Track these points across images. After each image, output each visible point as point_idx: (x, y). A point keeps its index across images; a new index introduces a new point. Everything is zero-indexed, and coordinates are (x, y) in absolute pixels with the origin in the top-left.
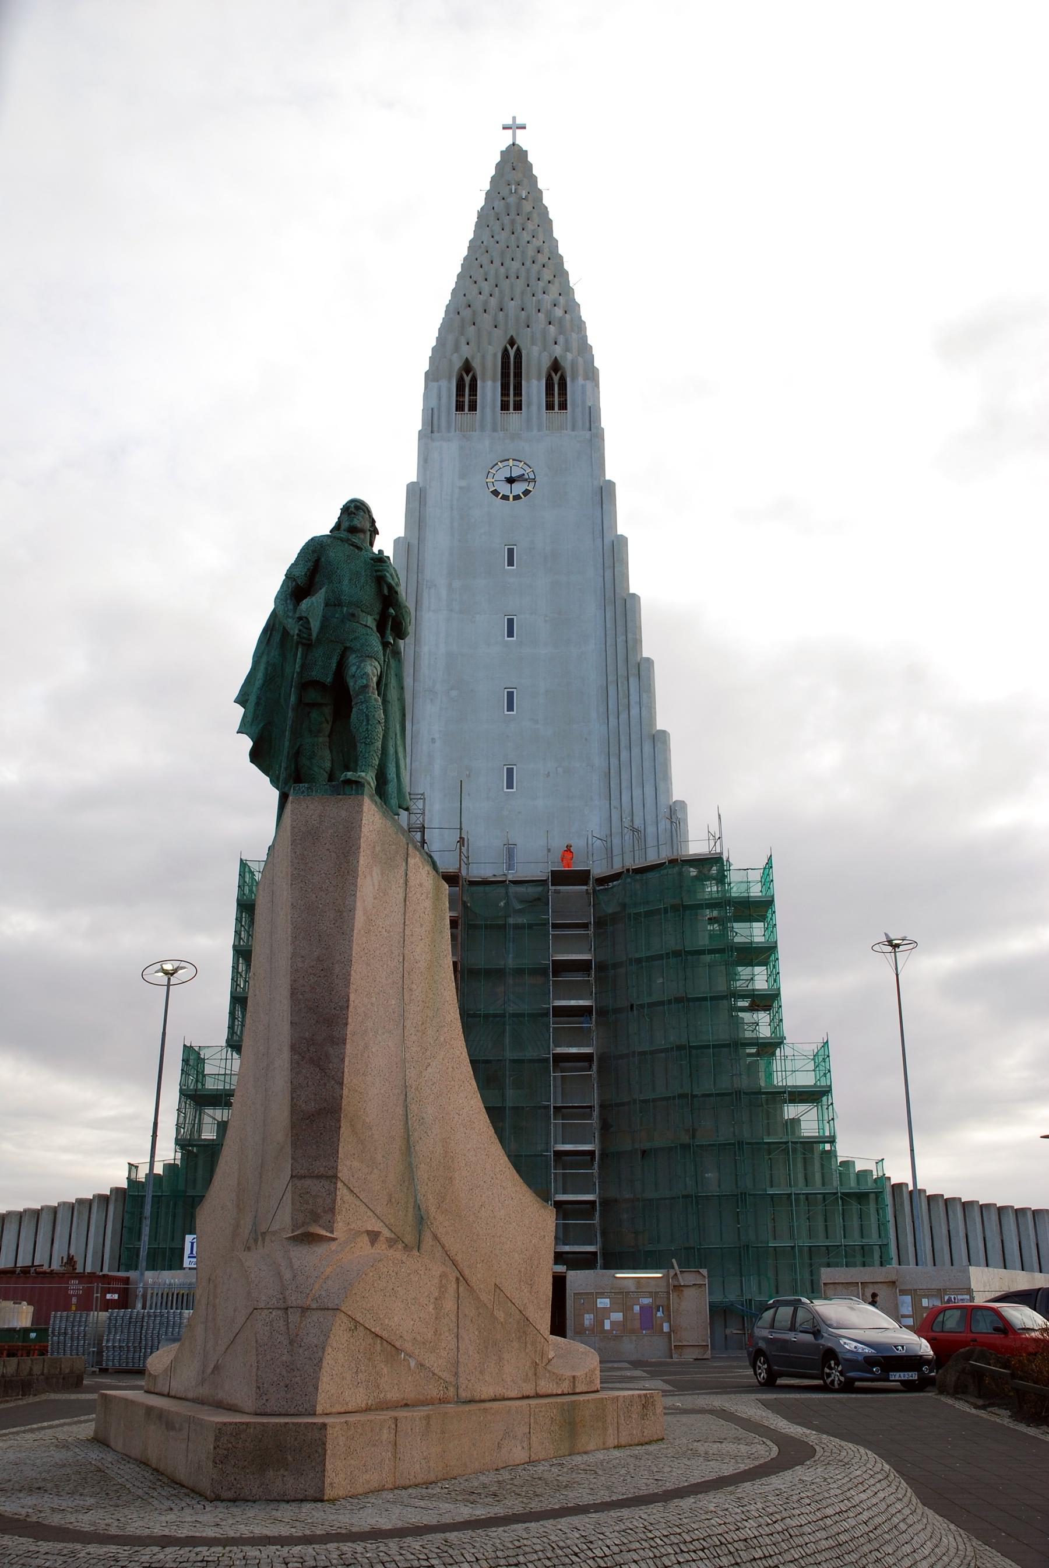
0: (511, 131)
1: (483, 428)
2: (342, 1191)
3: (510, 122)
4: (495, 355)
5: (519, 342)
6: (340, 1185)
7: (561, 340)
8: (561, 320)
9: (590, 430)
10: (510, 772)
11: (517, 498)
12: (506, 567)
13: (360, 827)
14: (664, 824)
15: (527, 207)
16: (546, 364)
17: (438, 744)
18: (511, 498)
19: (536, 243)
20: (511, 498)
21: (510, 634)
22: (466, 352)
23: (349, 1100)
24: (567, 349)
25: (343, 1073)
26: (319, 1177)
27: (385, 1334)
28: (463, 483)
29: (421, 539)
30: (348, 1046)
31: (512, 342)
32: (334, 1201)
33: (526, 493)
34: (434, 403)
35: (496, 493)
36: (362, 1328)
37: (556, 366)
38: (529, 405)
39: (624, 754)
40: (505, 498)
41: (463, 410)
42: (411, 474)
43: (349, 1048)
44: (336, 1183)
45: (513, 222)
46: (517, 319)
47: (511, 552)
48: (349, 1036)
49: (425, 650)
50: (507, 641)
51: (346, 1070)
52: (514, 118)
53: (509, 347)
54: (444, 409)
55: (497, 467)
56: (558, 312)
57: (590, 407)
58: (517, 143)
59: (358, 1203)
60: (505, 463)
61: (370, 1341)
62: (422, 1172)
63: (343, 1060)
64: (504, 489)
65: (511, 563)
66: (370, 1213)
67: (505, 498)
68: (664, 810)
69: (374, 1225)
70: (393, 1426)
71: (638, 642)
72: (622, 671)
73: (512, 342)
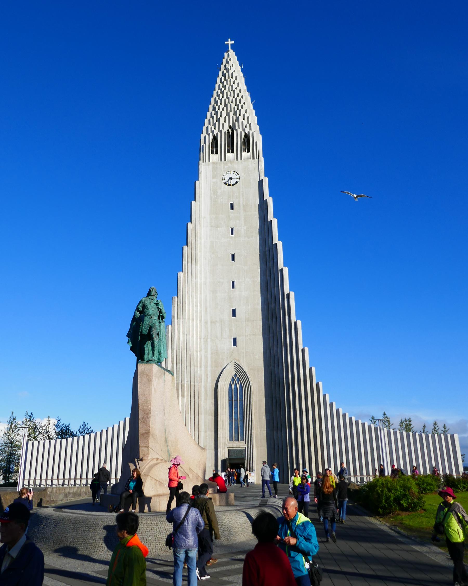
2: (150, 450)
4: (225, 132)
6: (149, 448)
9: (258, 159)
10: (233, 283)
11: (233, 185)
13: (153, 370)
16: (243, 135)
19: (238, 89)
20: (231, 184)
23: (151, 430)
24: (251, 129)
25: (150, 425)
26: (145, 447)
27: (159, 480)
30: (151, 419)
32: (148, 452)
33: (237, 183)
35: (226, 183)
36: (154, 479)
37: (247, 136)
39: (272, 275)
40: (229, 185)
41: (213, 154)
43: (151, 419)
44: (149, 448)
45: (230, 80)
46: (233, 117)
48: (151, 416)
50: (231, 237)
51: (150, 424)
57: (258, 150)
59: (154, 452)
61: (155, 481)
62: (170, 444)
63: (150, 422)
66: (157, 454)
69: (158, 456)
70: (159, 498)
73: (230, 127)
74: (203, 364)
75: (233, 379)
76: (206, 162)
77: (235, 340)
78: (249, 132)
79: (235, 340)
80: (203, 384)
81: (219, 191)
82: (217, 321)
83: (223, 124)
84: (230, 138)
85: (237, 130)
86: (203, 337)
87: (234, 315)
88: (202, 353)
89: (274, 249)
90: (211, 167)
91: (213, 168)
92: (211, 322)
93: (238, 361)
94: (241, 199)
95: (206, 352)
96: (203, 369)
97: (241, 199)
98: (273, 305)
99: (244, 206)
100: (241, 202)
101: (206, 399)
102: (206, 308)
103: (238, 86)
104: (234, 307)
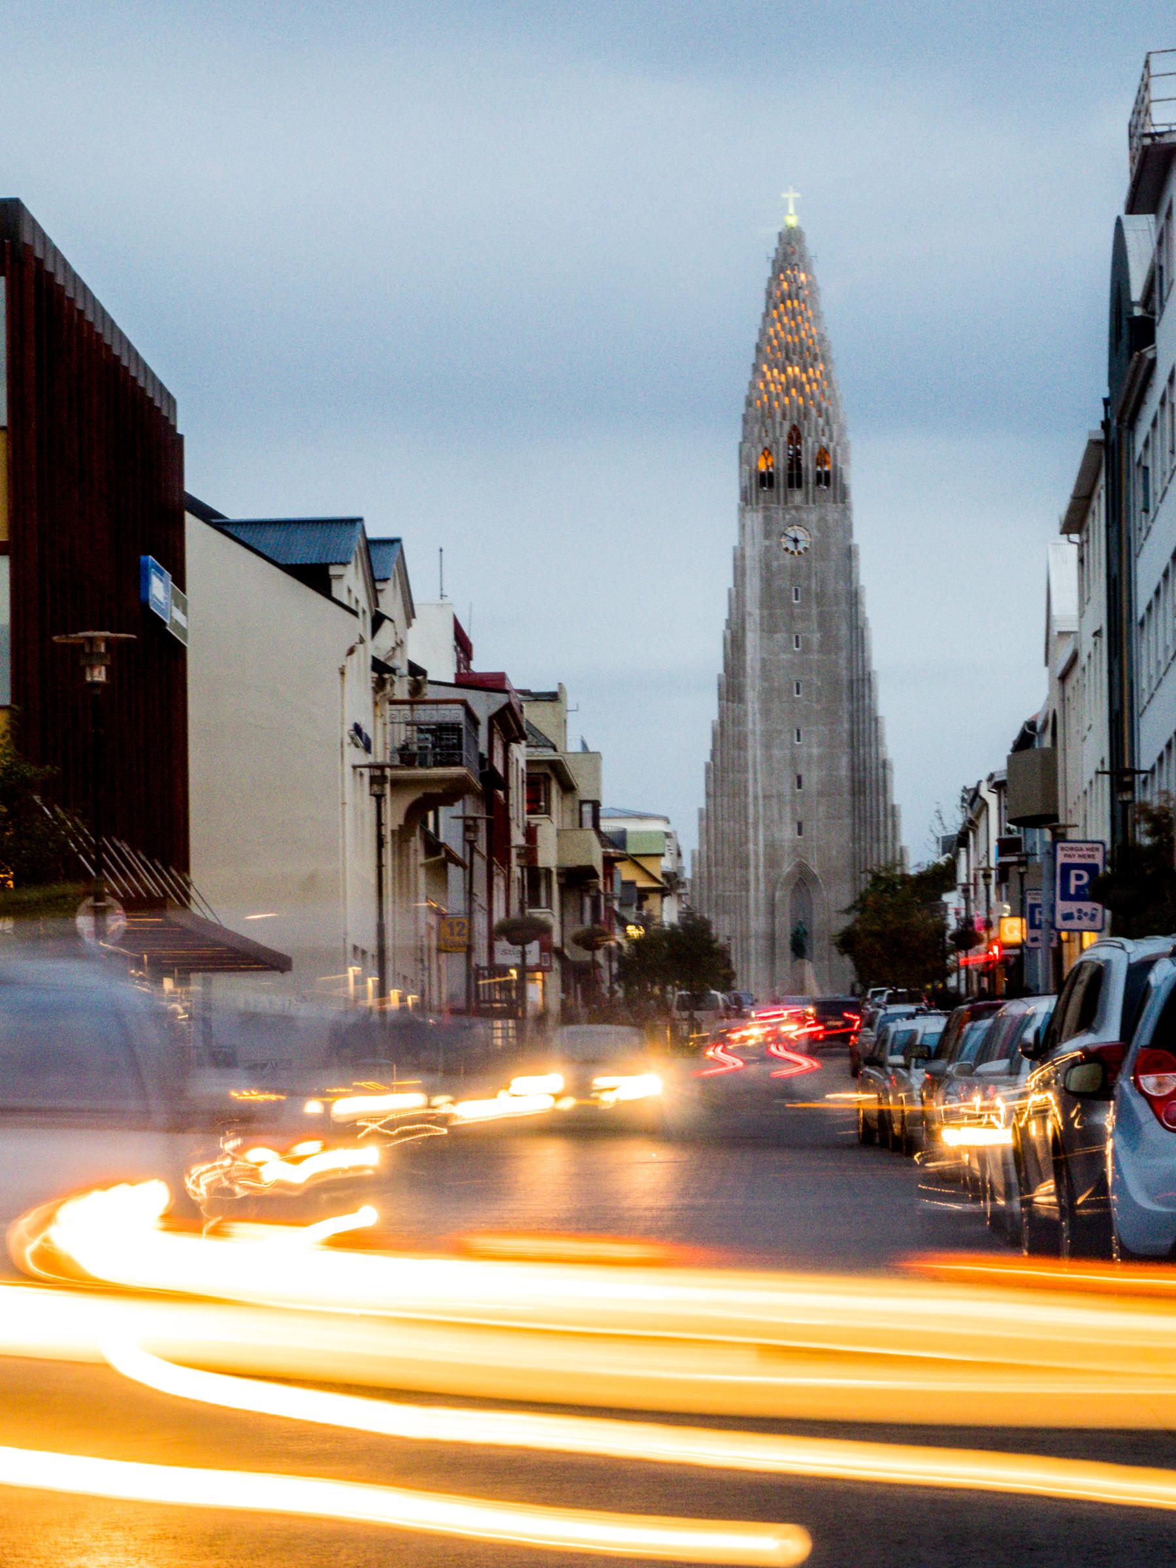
1: (778, 499)
12: (795, 602)
14: (881, 770)
17: (758, 716)
21: (797, 646)
24: (831, 439)
28: (767, 543)
29: (743, 584)
34: (748, 482)
38: (807, 483)
39: (861, 726)
42: (735, 541)
49: (749, 657)
54: (754, 486)
64: (791, 546)
67: (792, 553)
68: (880, 762)
72: (860, 673)
73: (794, 428)
74: (752, 862)
76: (752, 505)
78: (828, 446)
79: (800, 825)
80: (752, 893)
81: (775, 564)
82: (772, 796)
83: (781, 424)
84: (795, 462)
85: (806, 442)
86: (751, 820)
87: (799, 787)
88: (751, 846)
89: (866, 682)
90: (760, 515)
91: (765, 517)
92: (765, 797)
93: (805, 858)
94: (814, 581)
95: (756, 844)
96: (752, 869)
97: (814, 581)
98: (862, 774)
99: (817, 594)
100: (813, 586)
101: (757, 915)
102: (755, 773)
104: (799, 773)
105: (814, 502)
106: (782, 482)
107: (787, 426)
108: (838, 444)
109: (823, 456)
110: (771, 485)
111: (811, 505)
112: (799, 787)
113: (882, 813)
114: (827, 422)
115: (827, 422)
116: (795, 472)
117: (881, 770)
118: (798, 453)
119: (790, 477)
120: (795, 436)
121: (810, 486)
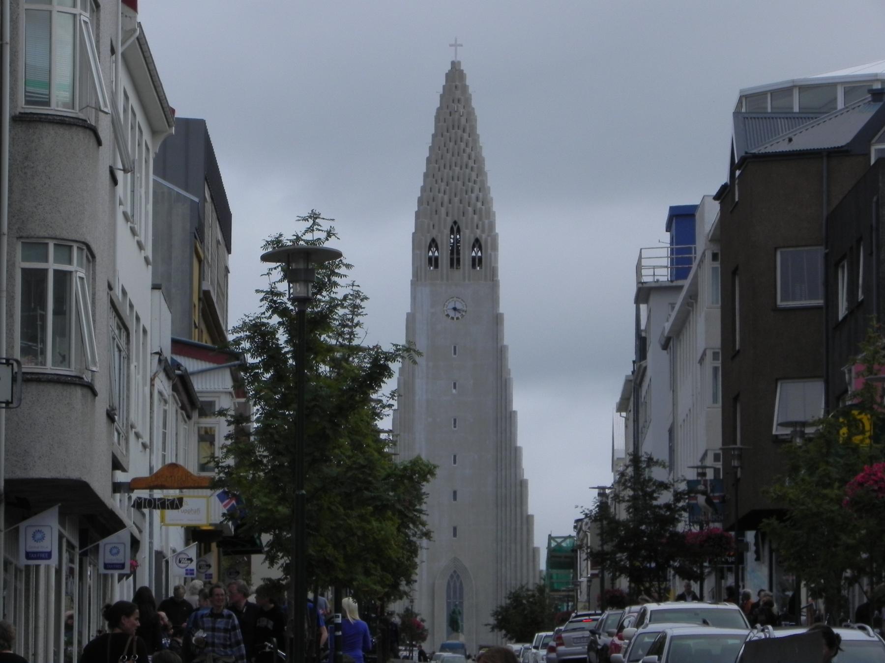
0: (453, 48)
3: (453, 42)
5: (460, 223)
7: (480, 226)
8: (481, 210)
9: (493, 280)
10: (455, 457)
15: (463, 120)
16: (472, 241)
18: (455, 319)
20: (455, 319)
22: (434, 233)
24: (483, 231)
31: (455, 223)
38: (464, 265)
47: (455, 348)
49: (417, 398)
52: (456, 40)
53: (454, 226)
55: (448, 301)
56: (479, 204)
57: (493, 267)
58: (458, 59)
60: (453, 299)
65: (455, 353)
67: (453, 318)
71: (511, 401)
73: (455, 223)
75: (452, 577)
77: (455, 529)
79: (455, 529)
87: (455, 498)
103: (467, 145)
105: (469, 280)
106: (445, 262)
107: (449, 223)
108: (488, 236)
109: (477, 243)
110: (436, 266)
111: (467, 281)
112: (455, 498)
113: (519, 522)
114: (480, 219)
115: (480, 219)
116: (455, 256)
117: (518, 488)
118: (457, 241)
119: (452, 260)
120: (455, 229)
121: (467, 267)
